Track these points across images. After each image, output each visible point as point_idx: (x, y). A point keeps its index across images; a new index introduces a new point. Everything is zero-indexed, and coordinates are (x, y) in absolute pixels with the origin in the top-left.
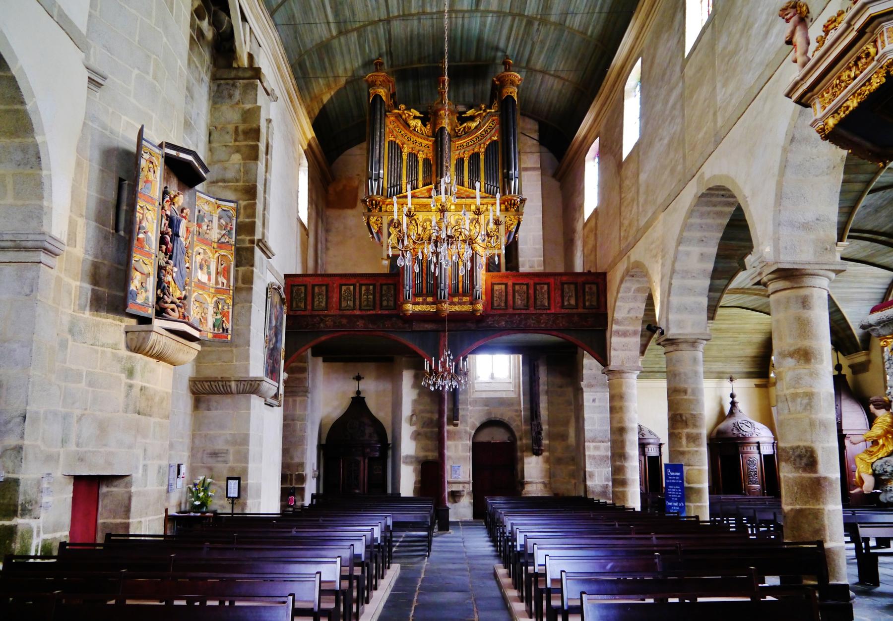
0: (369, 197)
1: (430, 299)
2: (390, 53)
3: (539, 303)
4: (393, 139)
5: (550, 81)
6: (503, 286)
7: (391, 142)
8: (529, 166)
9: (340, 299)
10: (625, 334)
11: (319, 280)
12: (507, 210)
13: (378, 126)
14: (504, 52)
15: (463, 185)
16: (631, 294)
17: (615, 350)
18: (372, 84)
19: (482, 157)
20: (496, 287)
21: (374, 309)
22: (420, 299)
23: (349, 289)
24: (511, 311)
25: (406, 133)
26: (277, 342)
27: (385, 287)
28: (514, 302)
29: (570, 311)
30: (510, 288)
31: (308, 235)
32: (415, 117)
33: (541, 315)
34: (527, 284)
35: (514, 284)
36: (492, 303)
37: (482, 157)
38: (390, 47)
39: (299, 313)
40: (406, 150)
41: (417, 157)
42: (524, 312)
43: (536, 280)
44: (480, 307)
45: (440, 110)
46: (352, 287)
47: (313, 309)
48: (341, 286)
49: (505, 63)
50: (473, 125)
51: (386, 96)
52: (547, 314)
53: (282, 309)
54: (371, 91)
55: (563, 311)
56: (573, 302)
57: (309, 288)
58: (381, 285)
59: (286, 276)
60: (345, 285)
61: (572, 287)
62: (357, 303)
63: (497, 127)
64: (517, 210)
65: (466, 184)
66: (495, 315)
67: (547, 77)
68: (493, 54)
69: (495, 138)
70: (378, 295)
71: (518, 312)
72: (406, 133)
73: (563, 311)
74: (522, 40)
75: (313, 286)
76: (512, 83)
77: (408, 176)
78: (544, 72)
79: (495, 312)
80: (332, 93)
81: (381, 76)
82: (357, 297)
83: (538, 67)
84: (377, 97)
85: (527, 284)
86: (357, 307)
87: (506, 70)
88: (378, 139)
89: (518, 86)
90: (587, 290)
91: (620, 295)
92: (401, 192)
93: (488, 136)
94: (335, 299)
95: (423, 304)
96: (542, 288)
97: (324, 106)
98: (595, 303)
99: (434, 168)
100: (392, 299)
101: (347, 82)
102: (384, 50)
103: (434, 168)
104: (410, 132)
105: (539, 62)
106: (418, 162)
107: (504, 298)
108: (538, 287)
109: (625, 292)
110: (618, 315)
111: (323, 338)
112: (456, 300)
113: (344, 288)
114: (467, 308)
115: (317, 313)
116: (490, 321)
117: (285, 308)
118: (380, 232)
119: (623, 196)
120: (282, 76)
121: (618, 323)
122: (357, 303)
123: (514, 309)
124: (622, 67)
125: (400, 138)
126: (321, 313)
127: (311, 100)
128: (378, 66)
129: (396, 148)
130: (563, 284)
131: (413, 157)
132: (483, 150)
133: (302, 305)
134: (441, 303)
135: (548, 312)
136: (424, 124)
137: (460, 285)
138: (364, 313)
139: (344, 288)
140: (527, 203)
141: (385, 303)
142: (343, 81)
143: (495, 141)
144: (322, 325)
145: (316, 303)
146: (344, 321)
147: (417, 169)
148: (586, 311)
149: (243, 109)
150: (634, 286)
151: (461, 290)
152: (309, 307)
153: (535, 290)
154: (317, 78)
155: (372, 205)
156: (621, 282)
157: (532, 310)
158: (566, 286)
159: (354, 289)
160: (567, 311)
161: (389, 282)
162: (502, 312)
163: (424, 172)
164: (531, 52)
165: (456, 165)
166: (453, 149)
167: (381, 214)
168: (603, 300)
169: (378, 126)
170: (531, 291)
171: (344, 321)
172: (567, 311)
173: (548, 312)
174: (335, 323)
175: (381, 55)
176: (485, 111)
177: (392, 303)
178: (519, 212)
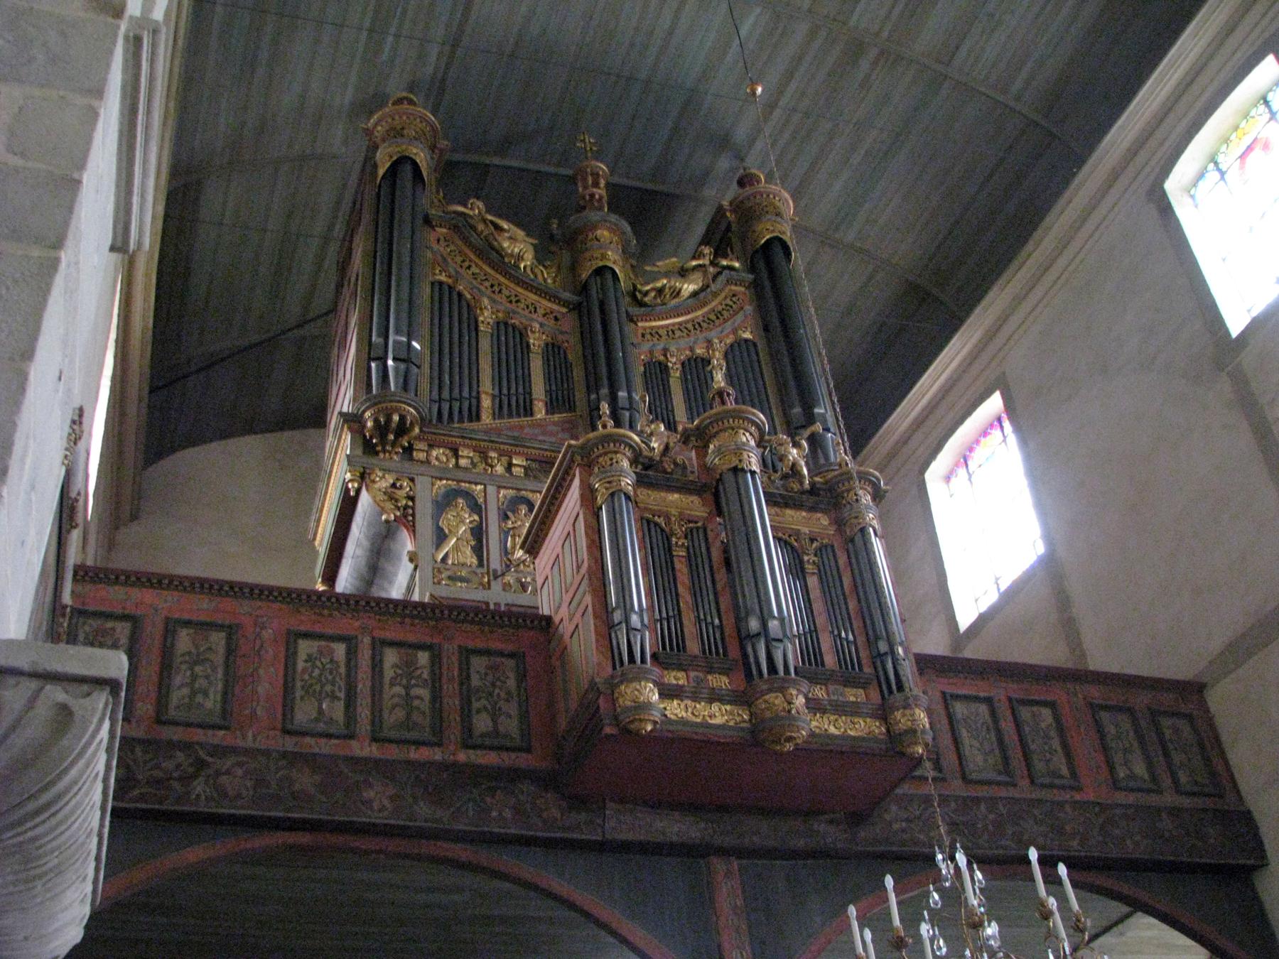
1: (720, 682)
3: (1039, 766)
4: (443, 278)
9: (288, 689)
11: (201, 606)
23: (332, 651)
27: (478, 663)
33: (1061, 805)
40: (487, 317)
46: (340, 650)
47: (159, 721)
48: (294, 637)
55: (1121, 797)
56: (1140, 769)
57: (153, 631)
60: (306, 635)
62: (364, 713)
69: (747, 335)
70: (450, 689)
71: (983, 792)
73: (1121, 797)
82: (364, 686)
85: (989, 701)
86: (364, 726)
94: (267, 683)
99: (578, 373)
102: (430, 70)
103: (578, 373)
108: (1025, 713)
113: (305, 647)
115: (175, 734)
122: (364, 713)
126: (199, 735)
130: (1094, 708)
137: (826, 643)
138: (394, 753)
139: (305, 648)
141: (482, 723)
143: (746, 341)
144: (199, 787)
145: (178, 695)
146: (305, 780)
148: (1186, 802)
157: (1024, 790)
159: (351, 653)
160: (1131, 798)
161: (495, 645)
167: (414, 469)
168: (1221, 769)
170: (1008, 726)
171: (305, 780)
172: (1131, 798)
173: (1078, 797)
174: (260, 782)
177: (510, 726)
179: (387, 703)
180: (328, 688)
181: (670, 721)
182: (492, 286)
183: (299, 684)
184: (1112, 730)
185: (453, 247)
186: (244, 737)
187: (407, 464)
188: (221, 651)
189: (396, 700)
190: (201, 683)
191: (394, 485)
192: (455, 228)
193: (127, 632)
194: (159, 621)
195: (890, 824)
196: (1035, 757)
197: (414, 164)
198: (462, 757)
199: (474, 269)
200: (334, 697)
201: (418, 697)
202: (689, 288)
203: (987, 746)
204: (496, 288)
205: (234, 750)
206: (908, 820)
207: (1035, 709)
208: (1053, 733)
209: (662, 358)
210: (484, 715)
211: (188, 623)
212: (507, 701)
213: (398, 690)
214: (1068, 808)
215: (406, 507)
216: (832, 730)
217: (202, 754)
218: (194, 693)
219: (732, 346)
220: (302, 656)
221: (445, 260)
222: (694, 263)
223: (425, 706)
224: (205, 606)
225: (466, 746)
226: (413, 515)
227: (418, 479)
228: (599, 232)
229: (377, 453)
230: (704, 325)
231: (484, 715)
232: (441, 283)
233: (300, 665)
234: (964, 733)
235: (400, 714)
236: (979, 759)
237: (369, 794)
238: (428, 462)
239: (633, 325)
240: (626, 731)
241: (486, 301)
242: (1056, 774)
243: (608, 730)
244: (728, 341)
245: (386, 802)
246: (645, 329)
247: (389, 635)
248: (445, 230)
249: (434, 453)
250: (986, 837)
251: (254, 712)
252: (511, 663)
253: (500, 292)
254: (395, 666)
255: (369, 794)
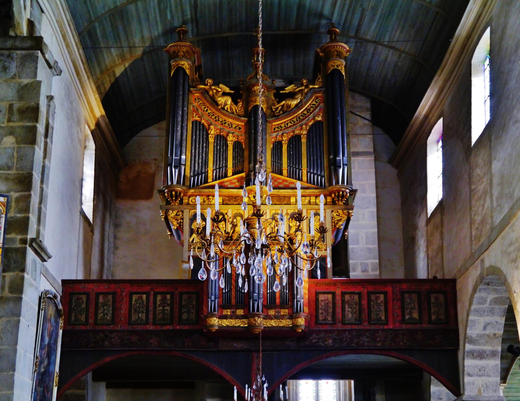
0: (168, 187)
1: (240, 312)
2: (195, 20)
3: (373, 316)
4: (197, 118)
5: (383, 53)
6: (330, 296)
7: (195, 123)
8: (361, 150)
10: (481, 355)
11: (104, 288)
12: (334, 203)
13: (180, 104)
14: (330, 19)
15: (281, 174)
16: (487, 305)
17: (469, 375)
18: (174, 56)
19: (304, 140)
20: (321, 297)
21: (172, 323)
22: (228, 312)
23: (142, 297)
24: (339, 326)
25: (215, 112)
26: (49, 364)
27: (185, 297)
28: (343, 315)
29: (412, 327)
30: (338, 298)
31: (92, 231)
32: (224, 94)
33: (377, 331)
34: (359, 294)
35: (343, 294)
36: (317, 317)
37: (304, 140)
38: (196, 14)
39: (78, 328)
40: (213, 132)
41: (226, 140)
42: (357, 327)
43: (371, 288)
44: (301, 321)
45: (254, 85)
46: (144, 296)
47: (96, 324)
48: (131, 295)
49: (331, 32)
50: (294, 103)
51: (191, 68)
52: (383, 330)
53: (57, 322)
54: (173, 63)
55: (404, 326)
56: (416, 315)
57: (93, 296)
58: (181, 294)
59: (63, 281)
61: (415, 297)
62: (151, 316)
63: (322, 105)
64: (346, 204)
65: (285, 172)
66: (320, 331)
67: (380, 48)
68: (316, 21)
69: (319, 119)
71: (349, 327)
72: (215, 112)
73: (404, 326)
74: (350, 6)
75: (97, 295)
76: (339, 55)
77: (215, 162)
78: (376, 43)
79: (321, 328)
80: (127, 65)
81: (185, 46)
82: (151, 308)
83: (368, 37)
84: (180, 70)
85: (359, 294)
86: (151, 321)
87: (332, 40)
88: (180, 119)
89: (345, 59)
90: (433, 300)
91: (473, 307)
92: (206, 181)
93: (311, 116)
95: (231, 317)
96: (377, 298)
97: (117, 80)
98: (442, 317)
99: (246, 153)
100: (193, 311)
101: (144, 53)
102: (189, 17)
103: (246, 153)
104: (219, 110)
105: (370, 32)
106: (227, 146)
107: (330, 310)
108: (373, 297)
109: (480, 303)
110: (472, 332)
111: (107, 359)
112: (272, 312)
114: (286, 323)
115: (100, 328)
116: (314, 339)
117: (61, 322)
118: (180, 228)
119: (473, 187)
120: (67, 46)
121: (472, 341)
122: (151, 316)
123: (343, 324)
124: (469, 37)
125: (206, 118)
126: (106, 328)
127: (102, 72)
128: (182, 35)
129: (200, 130)
130: (403, 293)
131: (221, 139)
132: (305, 132)
133: (83, 318)
134: (254, 316)
135: (386, 327)
136: (235, 102)
138: (159, 328)
139: (134, 297)
140: (358, 195)
141: (185, 316)
142: (139, 52)
143: (319, 121)
145: (100, 315)
147: (227, 154)
149: (19, 84)
150: (491, 297)
151: (278, 300)
152: (91, 321)
153: (369, 300)
154: (108, 48)
155: (172, 196)
156: (475, 290)
157: (366, 325)
158: (406, 295)
159: (148, 298)
162: (328, 328)
163: (234, 158)
164: (361, 20)
165: (273, 149)
166: (269, 131)
169: (180, 104)
170: (364, 302)
173: (386, 327)
175: (184, 23)
176: (307, 86)
177: (193, 316)
178: (348, 206)
179: (157, 312)
180: (141, 309)
181: (223, 326)
182: (216, 117)
183: (133, 309)
184: (408, 300)
185: (201, 102)
186: (118, 326)
187: (180, 206)
188: (111, 301)
189: (160, 311)
190: (106, 311)
191: (176, 215)
192: (202, 93)
193: (85, 298)
194: (94, 293)
195: (312, 340)
196: (372, 313)
197: (184, 70)
198: (178, 327)
199: (209, 111)
200: (142, 312)
201: (167, 310)
202: (294, 103)
203: (354, 311)
204: (217, 118)
205: (116, 331)
206: (318, 339)
207: (378, 295)
208: (383, 305)
209: (281, 139)
210: (185, 314)
211: (102, 293)
212: (192, 308)
213: (161, 308)
214: (380, 332)
215: (181, 222)
216: (274, 325)
217: (107, 333)
218: (104, 315)
219: (312, 125)
220: (134, 300)
221: (197, 110)
222: (298, 90)
223: (168, 312)
224: (106, 287)
225: (179, 325)
226: (183, 225)
227: (185, 211)
228: (255, 88)
229: (171, 203)
230: (301, 118)
231: (185, 314)
232: (196, 121)
233: (133, 303)
234: (347, 306)
235: (161, 315)
236: (350, 316)
237: (152, 341)
238: (188, 204)
239: (270, 124)
240: (209, 330)
241: (212, 127)
242: (380, 319)
243: (205, 331)
244: (311, 124)
245: (156, 343)
246: (275, 125)
247: (159, 290)
248: (197, 95)
249: (191, 199)
250: (346, 343)
251: (120, 319)
252: (194, 296)
253: (218, 120)
254: (160, 300)
255: (152, 341)
